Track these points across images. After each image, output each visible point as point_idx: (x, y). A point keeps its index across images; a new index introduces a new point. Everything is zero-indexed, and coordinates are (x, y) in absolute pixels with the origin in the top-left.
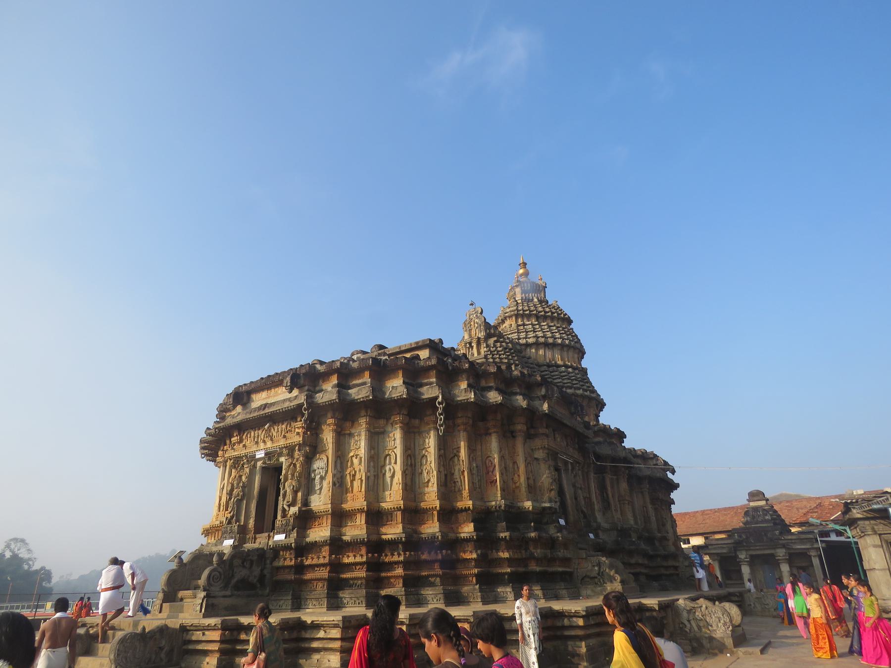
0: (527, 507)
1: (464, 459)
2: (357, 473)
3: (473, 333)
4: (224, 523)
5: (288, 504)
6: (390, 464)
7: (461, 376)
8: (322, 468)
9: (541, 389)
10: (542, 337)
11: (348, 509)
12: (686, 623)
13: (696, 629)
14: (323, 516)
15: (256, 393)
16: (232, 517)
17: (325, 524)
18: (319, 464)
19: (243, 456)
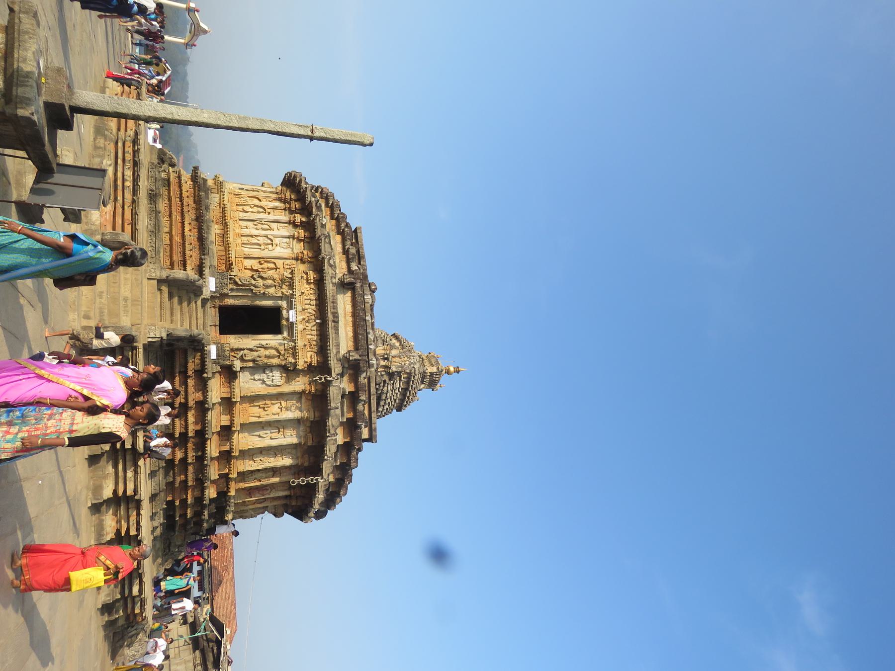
0: (227, 515)
1: (271, 481)
2: (266, 413)
3: (397, 359)
4: (232, 273)
5: (243, 356)
6: (271, 433)
7: (340, 474)
8: (273, 380)
9: (324, 507)
10: (386, 397)
11: (234, 409)
12: (134, 628)
13: (130, 634)
14: (230, 387)
15: (351, 297)
16: (236, 283)
17: (223, 390)
18: (277, 377)
19: (293, 292)
